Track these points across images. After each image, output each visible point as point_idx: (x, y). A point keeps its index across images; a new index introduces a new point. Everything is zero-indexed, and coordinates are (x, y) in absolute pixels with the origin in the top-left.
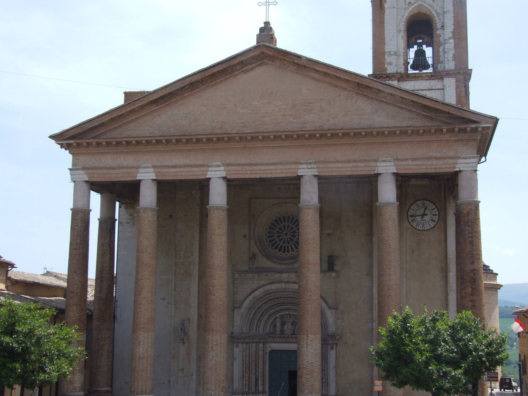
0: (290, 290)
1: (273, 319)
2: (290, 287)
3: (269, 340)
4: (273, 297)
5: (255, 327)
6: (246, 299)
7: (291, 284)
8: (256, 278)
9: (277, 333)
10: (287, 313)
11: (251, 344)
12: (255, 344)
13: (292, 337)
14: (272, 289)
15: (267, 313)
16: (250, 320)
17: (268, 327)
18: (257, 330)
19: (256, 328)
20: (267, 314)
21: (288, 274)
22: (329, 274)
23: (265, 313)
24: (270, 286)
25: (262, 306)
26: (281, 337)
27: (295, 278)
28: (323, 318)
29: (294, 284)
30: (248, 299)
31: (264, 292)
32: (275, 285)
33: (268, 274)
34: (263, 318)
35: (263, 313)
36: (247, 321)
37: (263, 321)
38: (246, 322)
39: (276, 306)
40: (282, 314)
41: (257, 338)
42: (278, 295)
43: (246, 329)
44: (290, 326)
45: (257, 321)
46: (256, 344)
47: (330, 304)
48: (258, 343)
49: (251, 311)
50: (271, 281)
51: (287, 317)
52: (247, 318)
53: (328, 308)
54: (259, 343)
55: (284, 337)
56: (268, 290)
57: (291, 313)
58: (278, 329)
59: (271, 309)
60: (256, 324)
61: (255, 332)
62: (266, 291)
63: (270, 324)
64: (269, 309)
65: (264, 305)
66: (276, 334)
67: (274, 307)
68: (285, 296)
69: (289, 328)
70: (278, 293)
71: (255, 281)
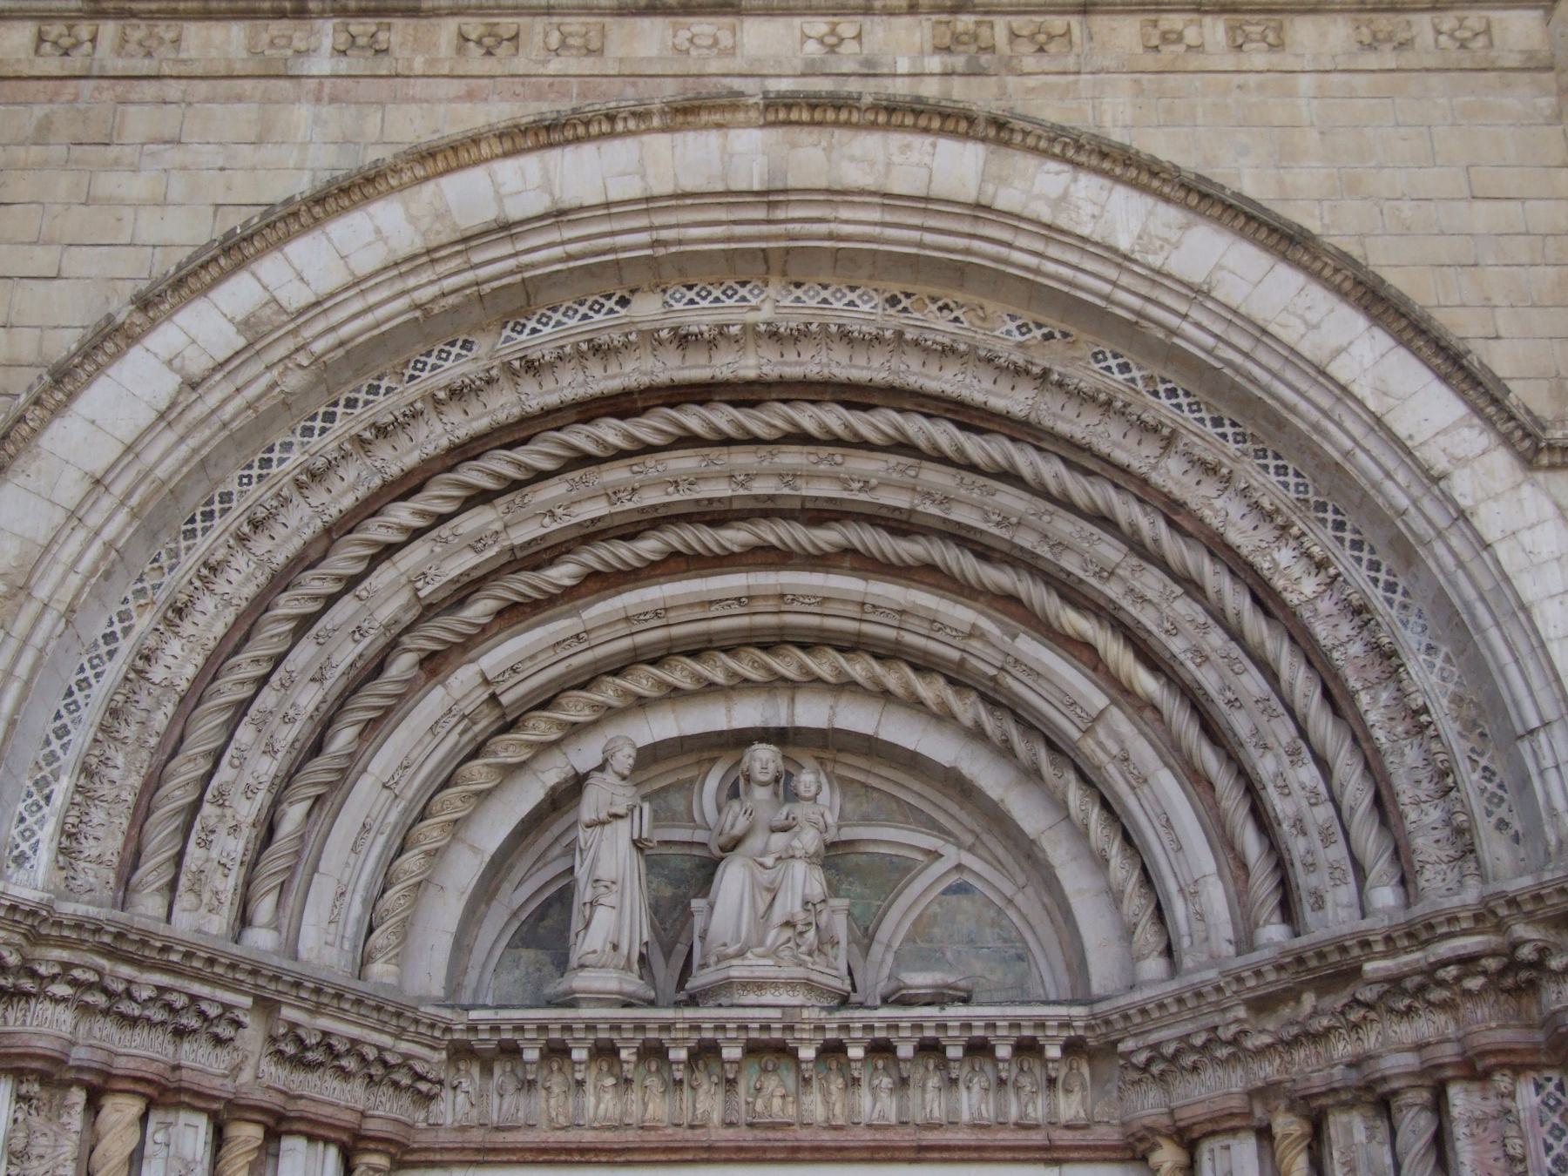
0: (857, 222)
1: (527, 795)
2: (854, 176)
3: (452, 1109)
4: (569, 386)
5: (235, 847)
6: (133, 339)
7: (870, 144)
8: (322, 64)
9: (582, 981)
10: (748, 713)
11: (121, 1111)
12: (192, 1134)
13: (832, 1050)
14: (559, 215)
15: (434, 664)
16: (160, 721)
17: (445, 912)
18: (264, 908)
19: (252, 866)
20: (434, 701)
21: (819, 26)
22: (1448, 21)
23: (403, 665)
24: (530, 164)
25: (377, 531)
26: (653, 1052)
27: (934, 63)
28: (1411, 640)
29: (921, 143)
30: (166, 338)
31: (430, 255)
32: (620, 152)
33: (507, 24)
34: (373, 728)
35: (376, 667)
36: (92, 712)
37: (365, 796)
38: (81, 737)
39: (591, 558)
40: (663, 726)
41: (253, 1035)
42: (652, 339)
43: (70, 841)
44: (805, 880)
45: (267, 768)
46: (219, 1139)
47: (1530, 395)
48: (247, 1134)
49: (189, 563)
50: (547, 108)
51: (734, 790)
52: (115, 670)
53: (1502, 460)
54: (277, 1127)
55: (706, 1052)
56: (505, 229)
57: (811, 713)
58: (603, 920)
59: (514, 614)
60: (248, 810)
61: (219, 923)
62: (467, 240)
63: (465, 870)
64: (480, 609)
65: (403, 514)
66: (569, 1001)
67: (563, 574)
68: (748, 365)
69: (789, 905)
70: (647, 308)
71: (303, 113)
